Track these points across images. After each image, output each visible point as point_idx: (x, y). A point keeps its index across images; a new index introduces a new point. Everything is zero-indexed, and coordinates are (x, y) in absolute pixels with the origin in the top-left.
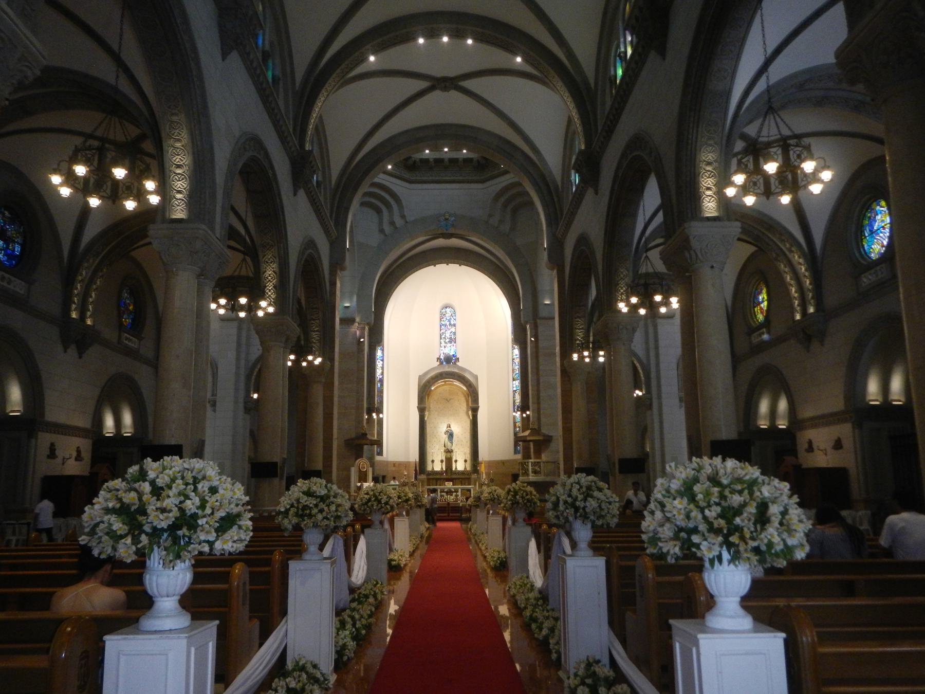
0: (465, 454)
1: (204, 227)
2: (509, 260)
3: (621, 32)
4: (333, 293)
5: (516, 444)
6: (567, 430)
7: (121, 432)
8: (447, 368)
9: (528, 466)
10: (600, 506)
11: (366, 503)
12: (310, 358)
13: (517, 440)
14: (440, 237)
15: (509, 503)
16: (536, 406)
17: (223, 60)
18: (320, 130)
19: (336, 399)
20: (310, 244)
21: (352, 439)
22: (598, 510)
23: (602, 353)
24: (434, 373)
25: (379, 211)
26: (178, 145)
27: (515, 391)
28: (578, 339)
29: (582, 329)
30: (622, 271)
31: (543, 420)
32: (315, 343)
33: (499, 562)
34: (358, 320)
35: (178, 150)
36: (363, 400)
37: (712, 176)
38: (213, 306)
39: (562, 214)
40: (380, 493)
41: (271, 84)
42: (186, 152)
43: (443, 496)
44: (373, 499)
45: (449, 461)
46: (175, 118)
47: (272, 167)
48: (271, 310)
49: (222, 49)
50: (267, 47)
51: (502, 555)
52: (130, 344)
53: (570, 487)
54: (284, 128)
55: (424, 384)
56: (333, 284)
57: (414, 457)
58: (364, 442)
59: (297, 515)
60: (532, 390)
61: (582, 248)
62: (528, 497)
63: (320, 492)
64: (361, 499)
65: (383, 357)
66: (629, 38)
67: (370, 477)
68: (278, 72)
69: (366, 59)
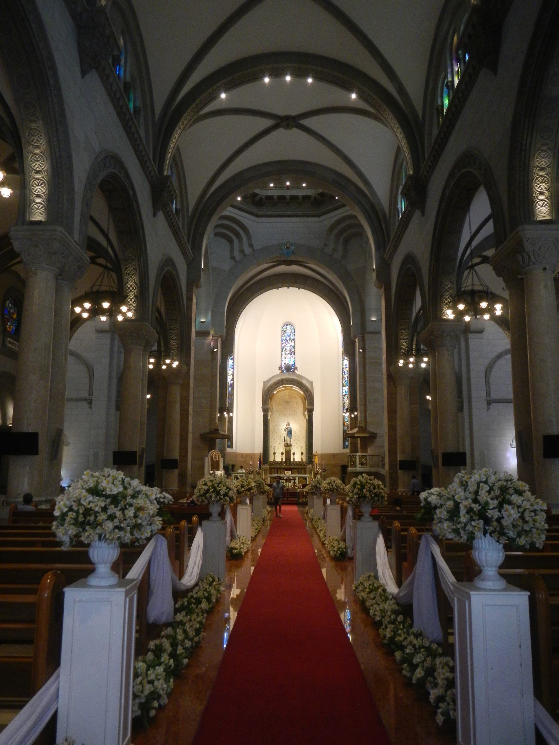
1: (60, 229)
2: (341, 284)
3: (449, 62)
4: (190, 307)
5: (345, 440)
6: (392, 428)
7: (6, 423)
8: (287, 376)
9: (356, 458)
10: (522, 517)
11: (204, 495)
12: (168, 361)
13: (346, 436)
14: (281, 264)
15: (356, 496)
16: (363, 407)
17: (83, 77)
18: (177, 162)
19: (191, 398)
20: (169, 262)
21: (206, 434)
22: (520, 523)
23: (426, 359)
25: (230, 241)
26: (37, 151)
27: (344, 396)
28: (402, 349)
29: (406, 339)
30: (446, 283)
31: (369, 419)
32: (174, 350)
33: (339, 552)
34: (212, 332)
35: (37, 156)
36: (216, 402)
37: (545, 181)
38: (78, 310)
39: (389, 240)
40: (219, 484)
41: (133, 115)
42: (45, 158)
44: (211, 490)
45: (288, 454)
46: (33, 125)
47: (133, 188)
48: (130, 315)
49: (81, 66)
50: (128, 79)
51: (342, 545)
52: (13, 347)
53: (475, 488)
54: (143, 153)
56: (190, 299)
57: (258, 449)
58: (215, 436)
59: (76, 522)
60: (360, 394)
61: (409, 266)
62: (375, 491)
63: (111, 490)
64: (199, 490)
65: (233, 365)
66: (456, 69)
68: (139, 104)
69: (217, 96)
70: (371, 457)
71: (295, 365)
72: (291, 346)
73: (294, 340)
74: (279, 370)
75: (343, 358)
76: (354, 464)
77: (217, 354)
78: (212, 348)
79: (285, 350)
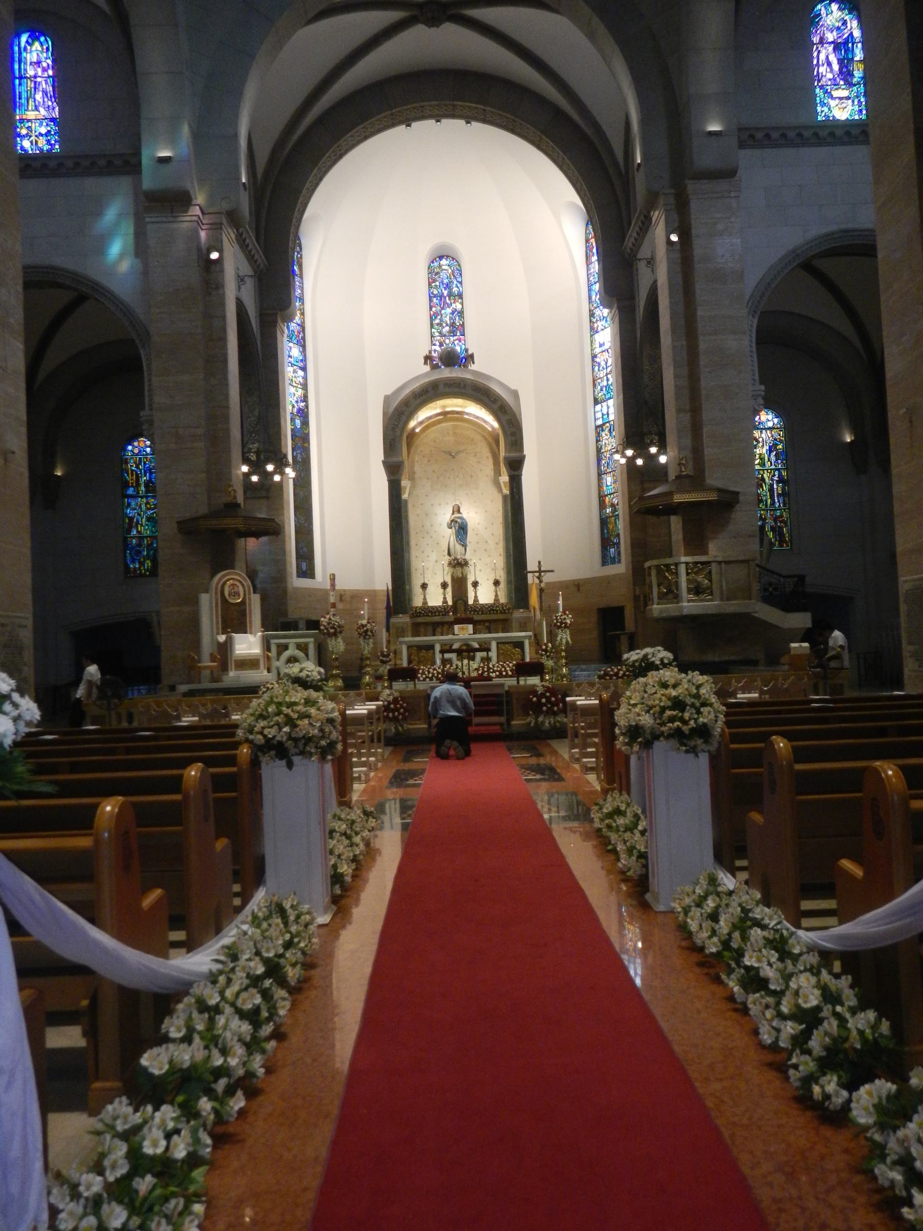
0: (494, 569)
5: (607, 541)
8: (446, 373)
9: (676, 574)
16: (687, 418)
24: (418, 384)
27: (599, 429)
31: (710, 452)
34: (200, 199)
36: (226, 418)
43: (450, 661)
45: (459, 585)
55: (396, 409)
57: (383, 580)
60: (676, 376)
65: (304, 360)
67: (256, 616)
70: (723, 565)
71: (466, 350)
72: (453, 313)
73: (460, 296)
74: (425, 363)
75: (592, 328)
76: (670, 591)
77: (222, 271)
78: (205, 251)
79: (440, 324)
